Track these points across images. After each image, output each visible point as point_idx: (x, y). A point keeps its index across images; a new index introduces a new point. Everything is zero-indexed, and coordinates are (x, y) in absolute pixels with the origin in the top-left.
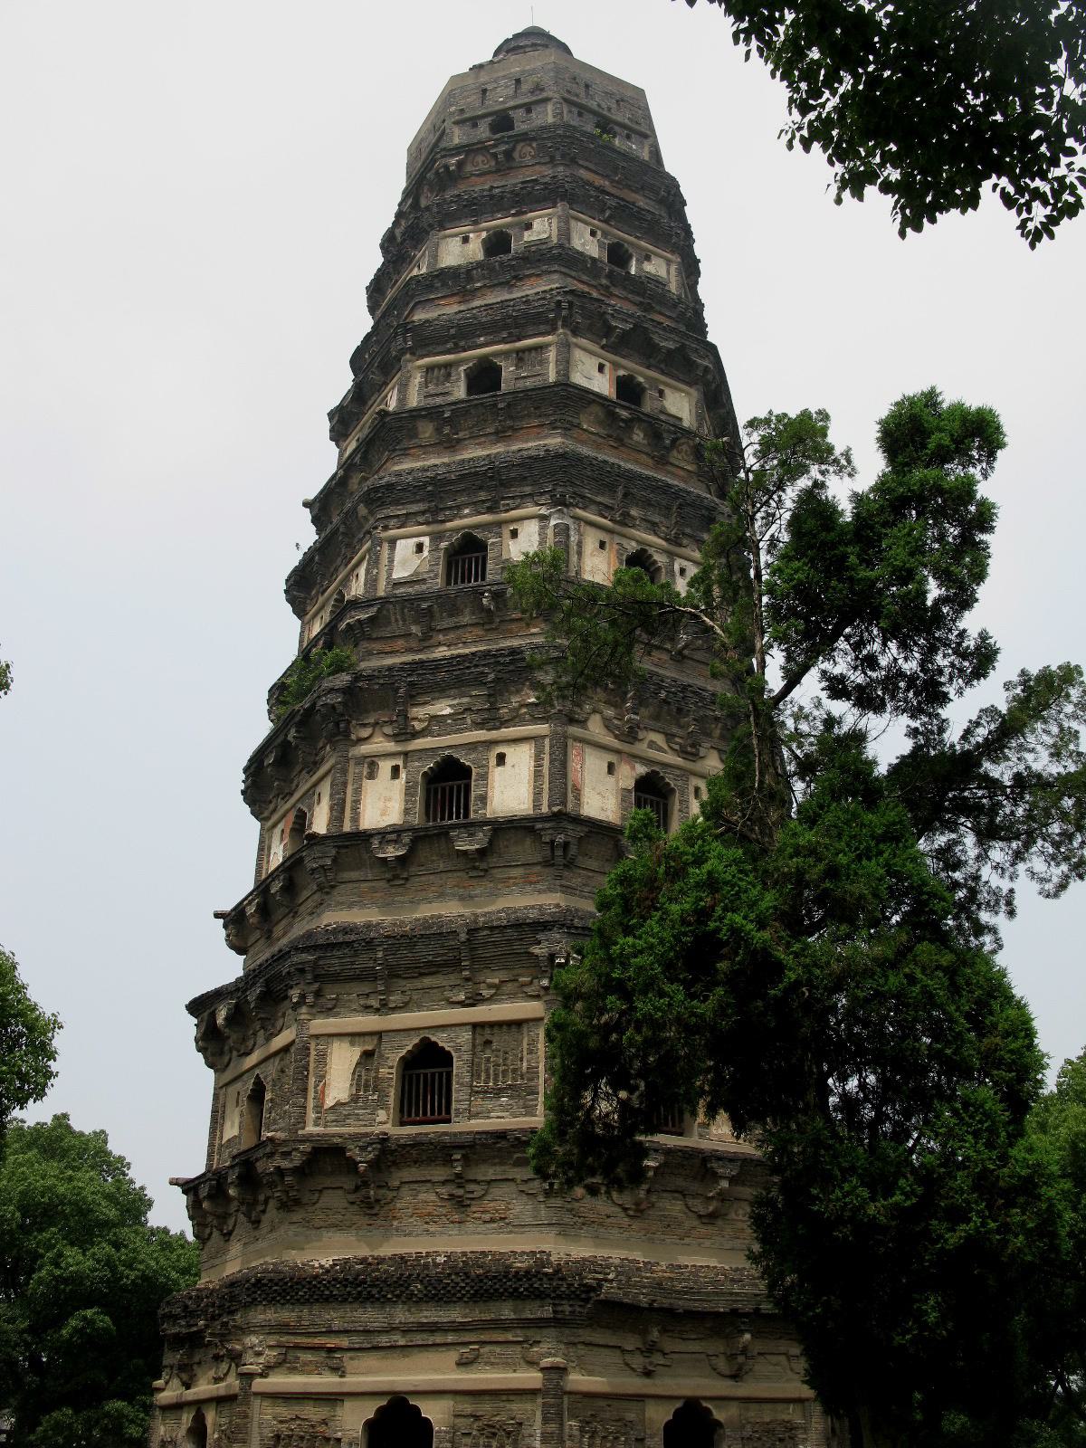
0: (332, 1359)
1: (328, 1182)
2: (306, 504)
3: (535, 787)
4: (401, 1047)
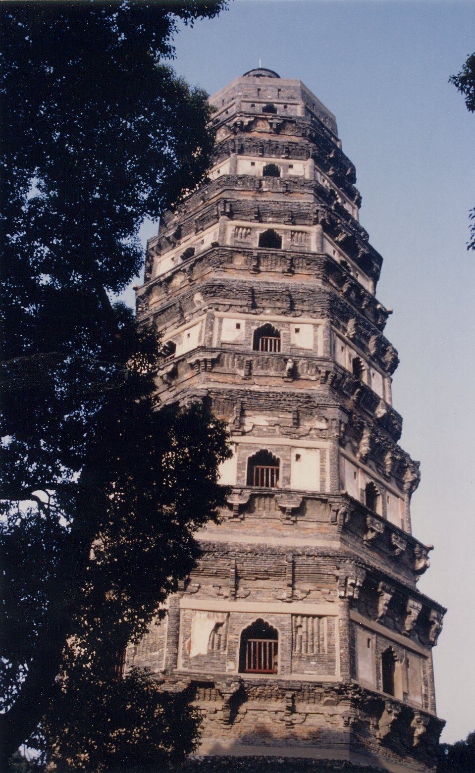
3: (321, 478)
4: (243, 623)
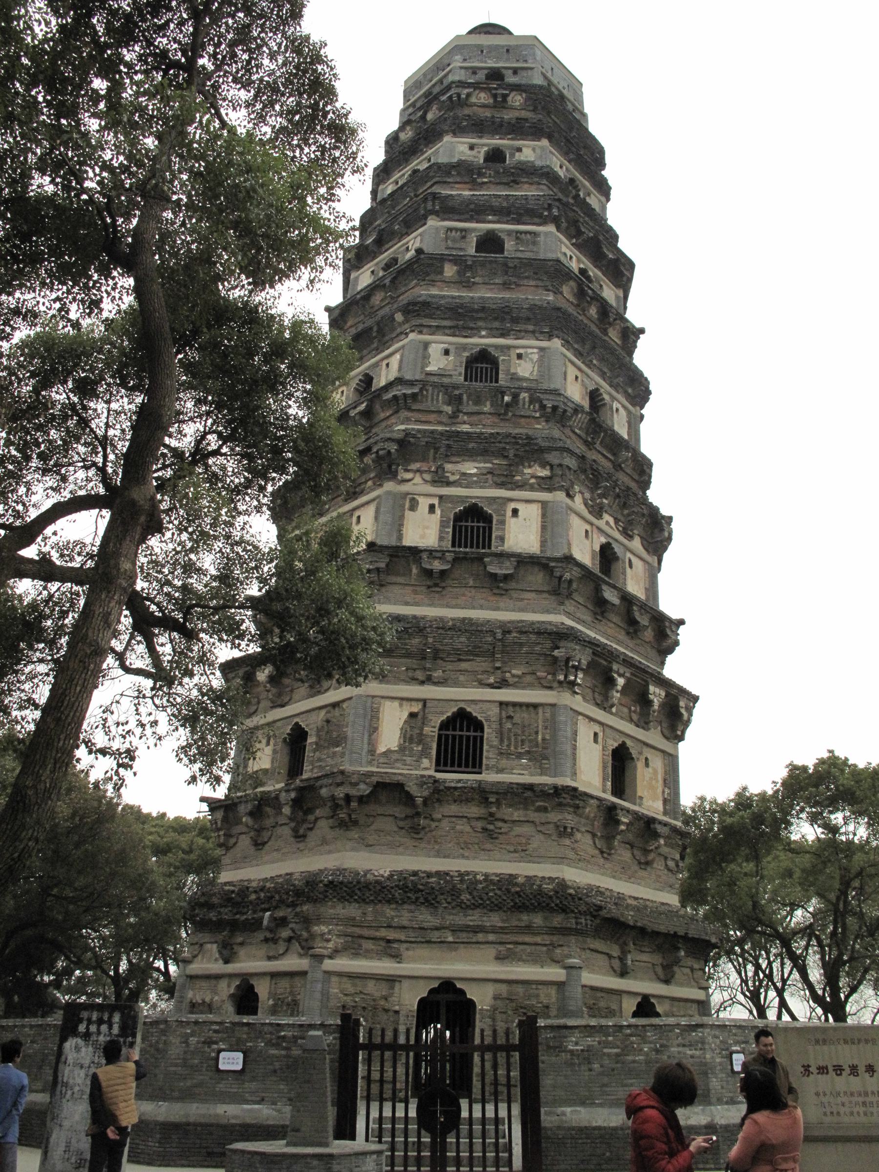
0: (389, 949)
1: (380, 810)
4: (442, 713)
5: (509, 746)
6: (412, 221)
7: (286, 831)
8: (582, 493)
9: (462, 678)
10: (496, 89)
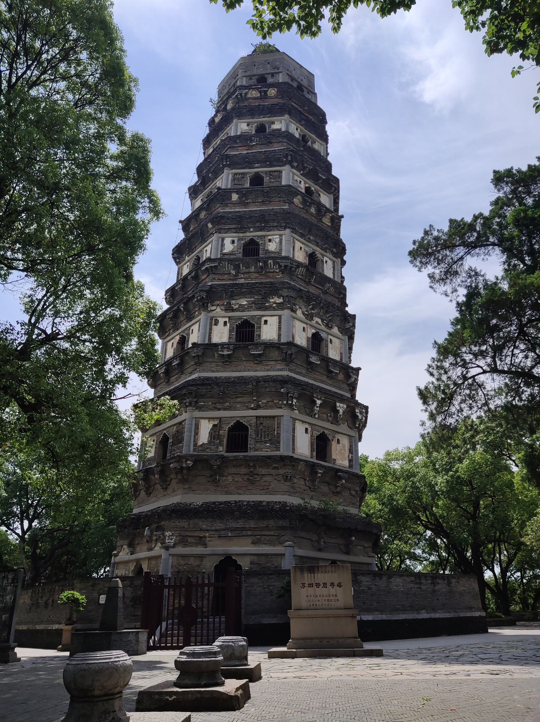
0: (201, 541)
2: (181, 222)
4: (228, 424)
5: (261, 438)
6: (217, 173)
7: (158, 486)
8: (301, 309)
9: (238, 406)
10: (260, 88)
